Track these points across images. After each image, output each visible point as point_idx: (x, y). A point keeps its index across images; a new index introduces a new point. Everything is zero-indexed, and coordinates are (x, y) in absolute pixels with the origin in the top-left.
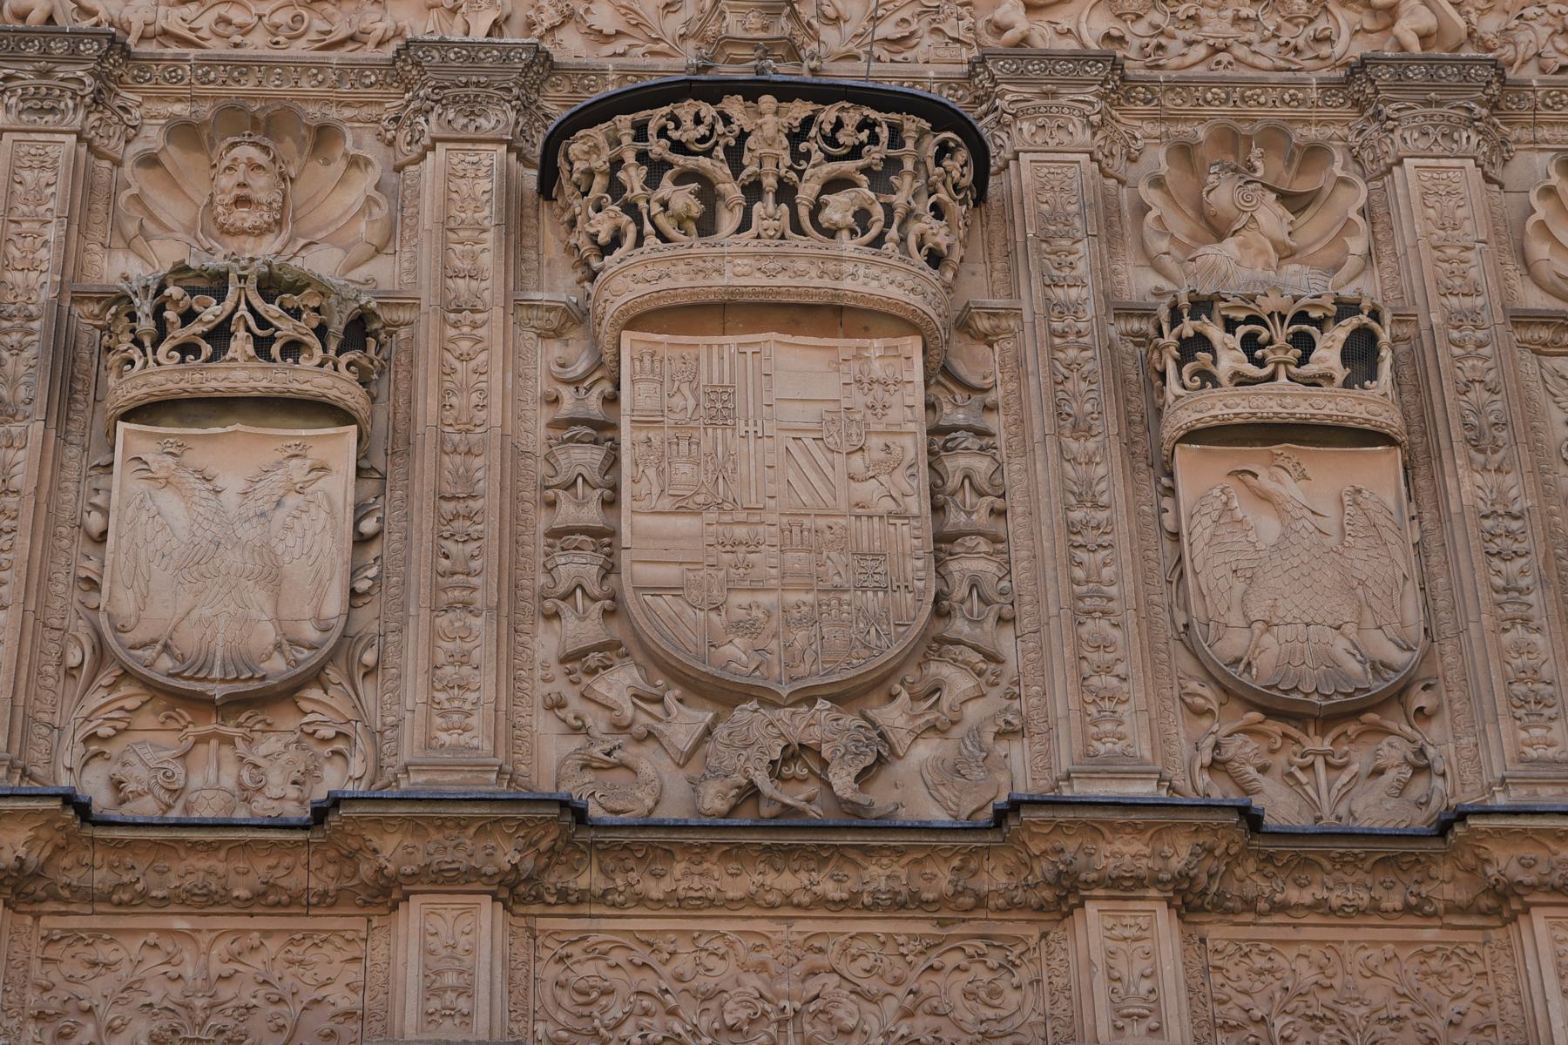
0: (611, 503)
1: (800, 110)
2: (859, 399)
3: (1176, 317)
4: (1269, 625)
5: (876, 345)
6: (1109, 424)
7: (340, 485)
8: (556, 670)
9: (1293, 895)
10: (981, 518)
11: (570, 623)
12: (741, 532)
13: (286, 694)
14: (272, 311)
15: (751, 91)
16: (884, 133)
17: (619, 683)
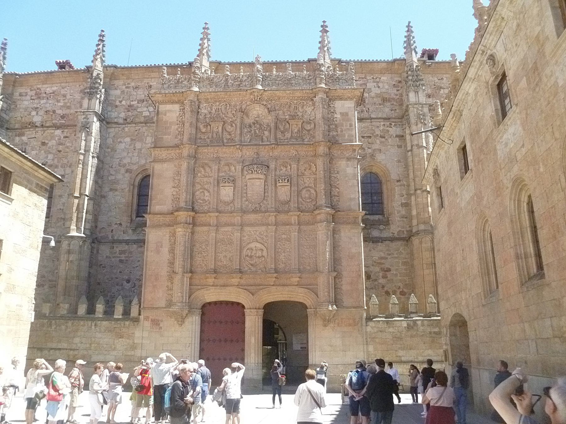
7: (232, 190)
17: (247, 203)
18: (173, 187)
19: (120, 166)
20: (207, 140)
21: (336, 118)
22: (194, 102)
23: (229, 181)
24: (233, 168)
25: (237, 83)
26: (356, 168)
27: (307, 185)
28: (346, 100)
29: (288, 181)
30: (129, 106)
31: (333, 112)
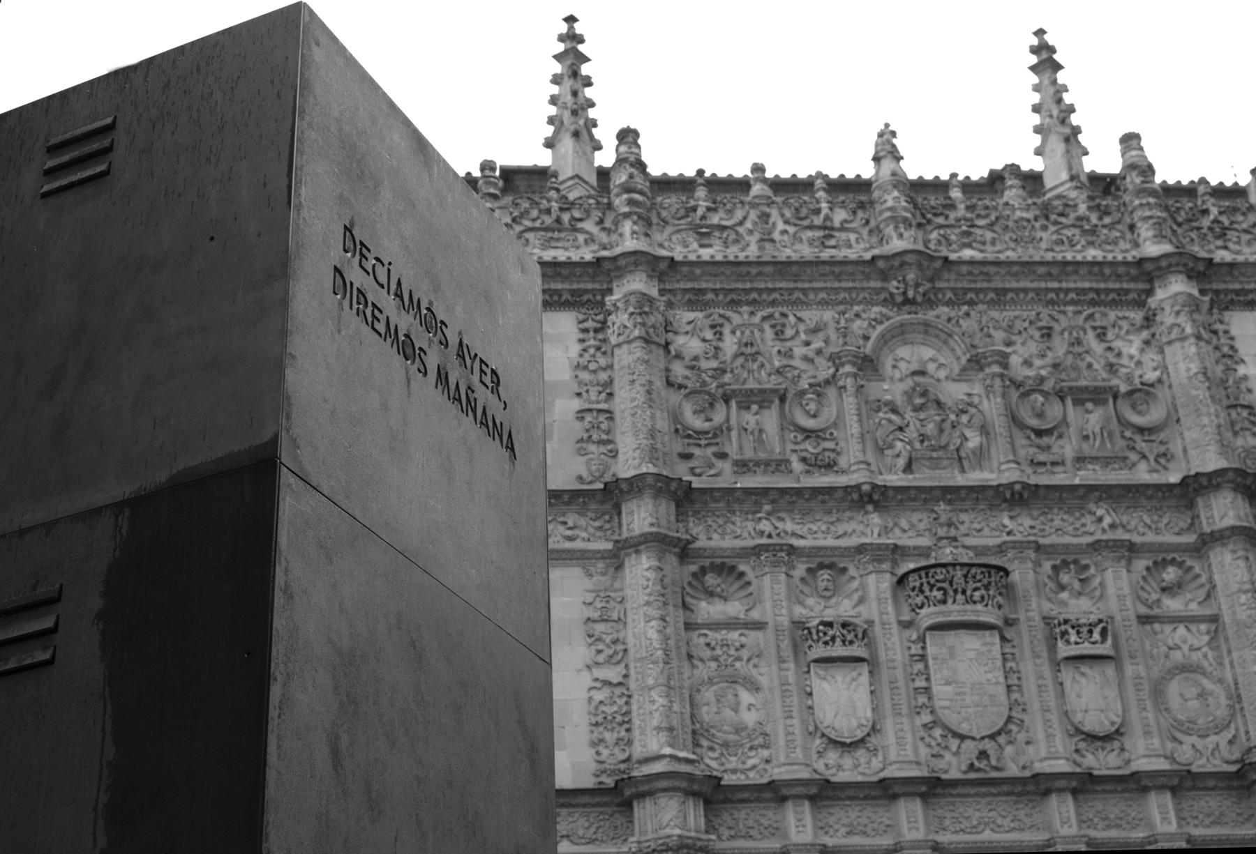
0: (928, 679)
1: (966, 569)
2: (984, 649)
3: (1060, 624)
4: (1086, 711)
5: (987, 633)
6: (1045, 654)
7: (865, 678)
8: (921, 728)
10: (1016, 682)
11: (923, 716)
12: (961, 690)
14: (845, 632)
16: (987, 575)
17: (938, 732)
18: (589, 667)
20: (719, 464)
21: (1245, 378)
22: (651, 300)
23: (850, 637)
25: (810, 234)
27: (1177, 656)
29: (1104, 633)
31: (1231, 357)
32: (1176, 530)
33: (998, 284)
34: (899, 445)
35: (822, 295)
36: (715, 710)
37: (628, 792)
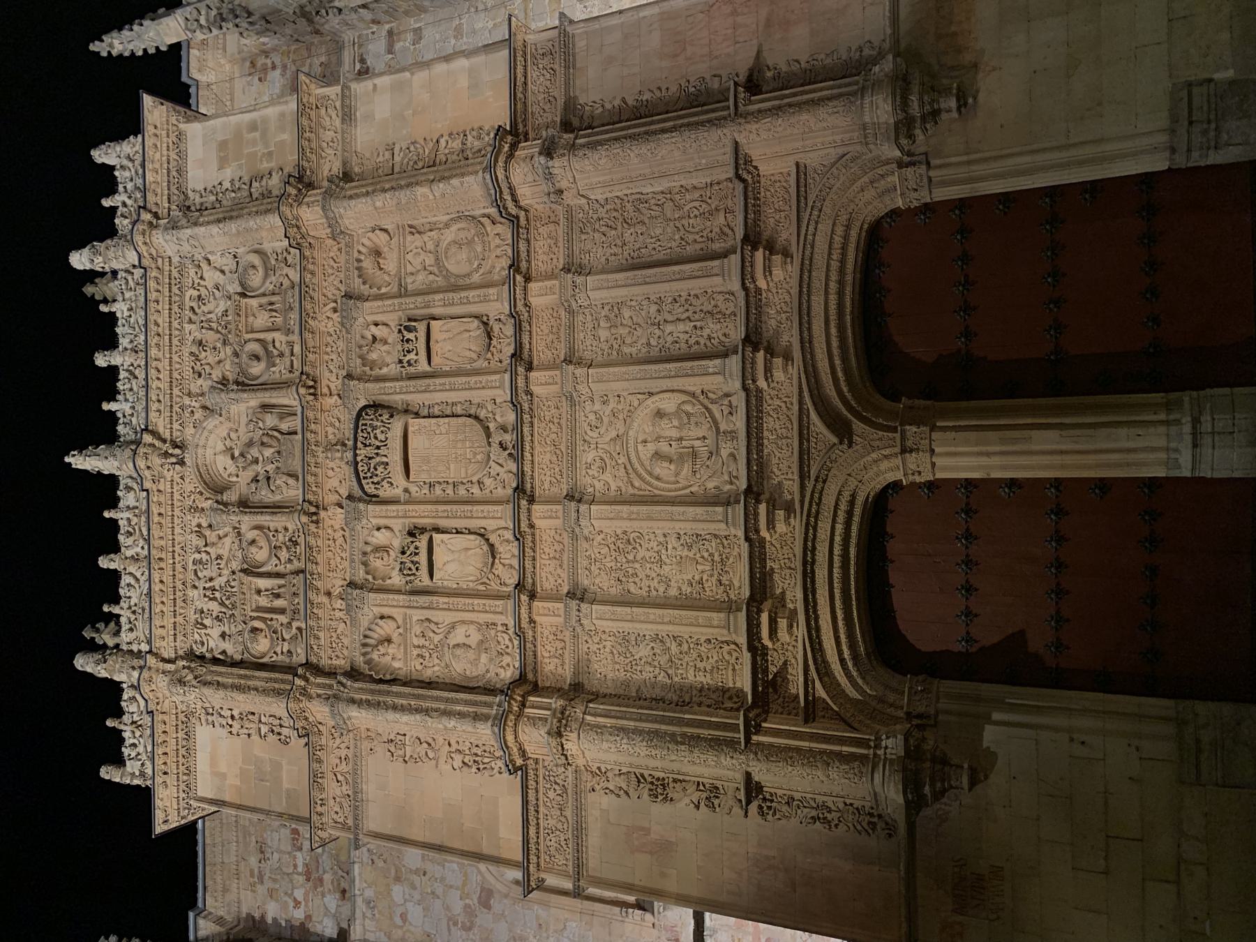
1: (359, 444)
6: (427, 381)
9: (528, 346)
10: (449, 408)
13: (492, 546)
14: (408, 553)
15: (356, 455)
19: (470, 929)
21: (232, 181)
23: (412, 548)
24: (381, 538)
26: (375, 86)
28: (182, 155)
29: (408, 329)
30: (308, 880)
32: (338, 253)
33: (164, 385)
34: (278, 482)
35: (178, 530)
36: (469, 665)
37: (519, 762)
